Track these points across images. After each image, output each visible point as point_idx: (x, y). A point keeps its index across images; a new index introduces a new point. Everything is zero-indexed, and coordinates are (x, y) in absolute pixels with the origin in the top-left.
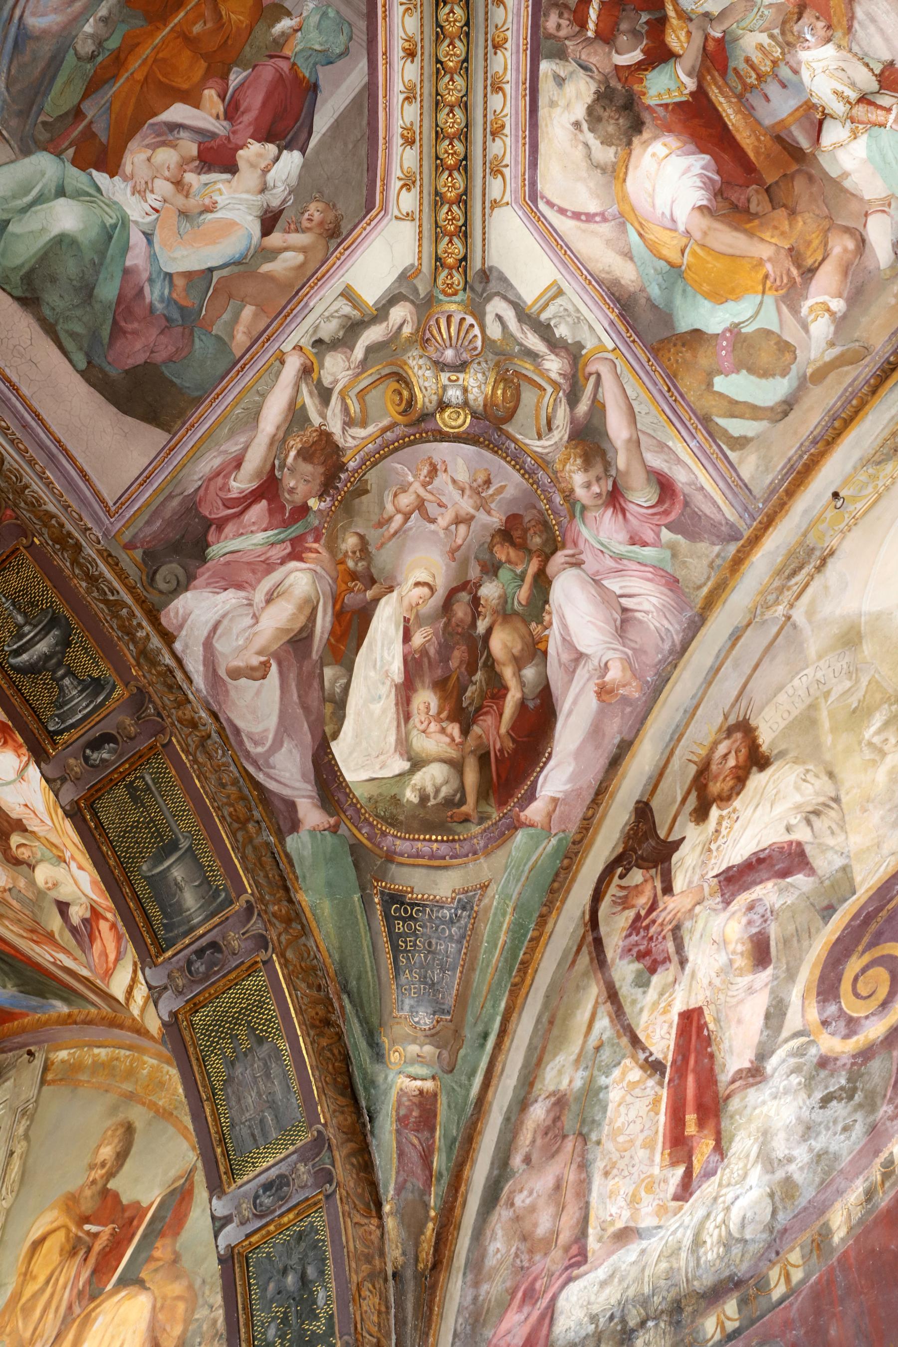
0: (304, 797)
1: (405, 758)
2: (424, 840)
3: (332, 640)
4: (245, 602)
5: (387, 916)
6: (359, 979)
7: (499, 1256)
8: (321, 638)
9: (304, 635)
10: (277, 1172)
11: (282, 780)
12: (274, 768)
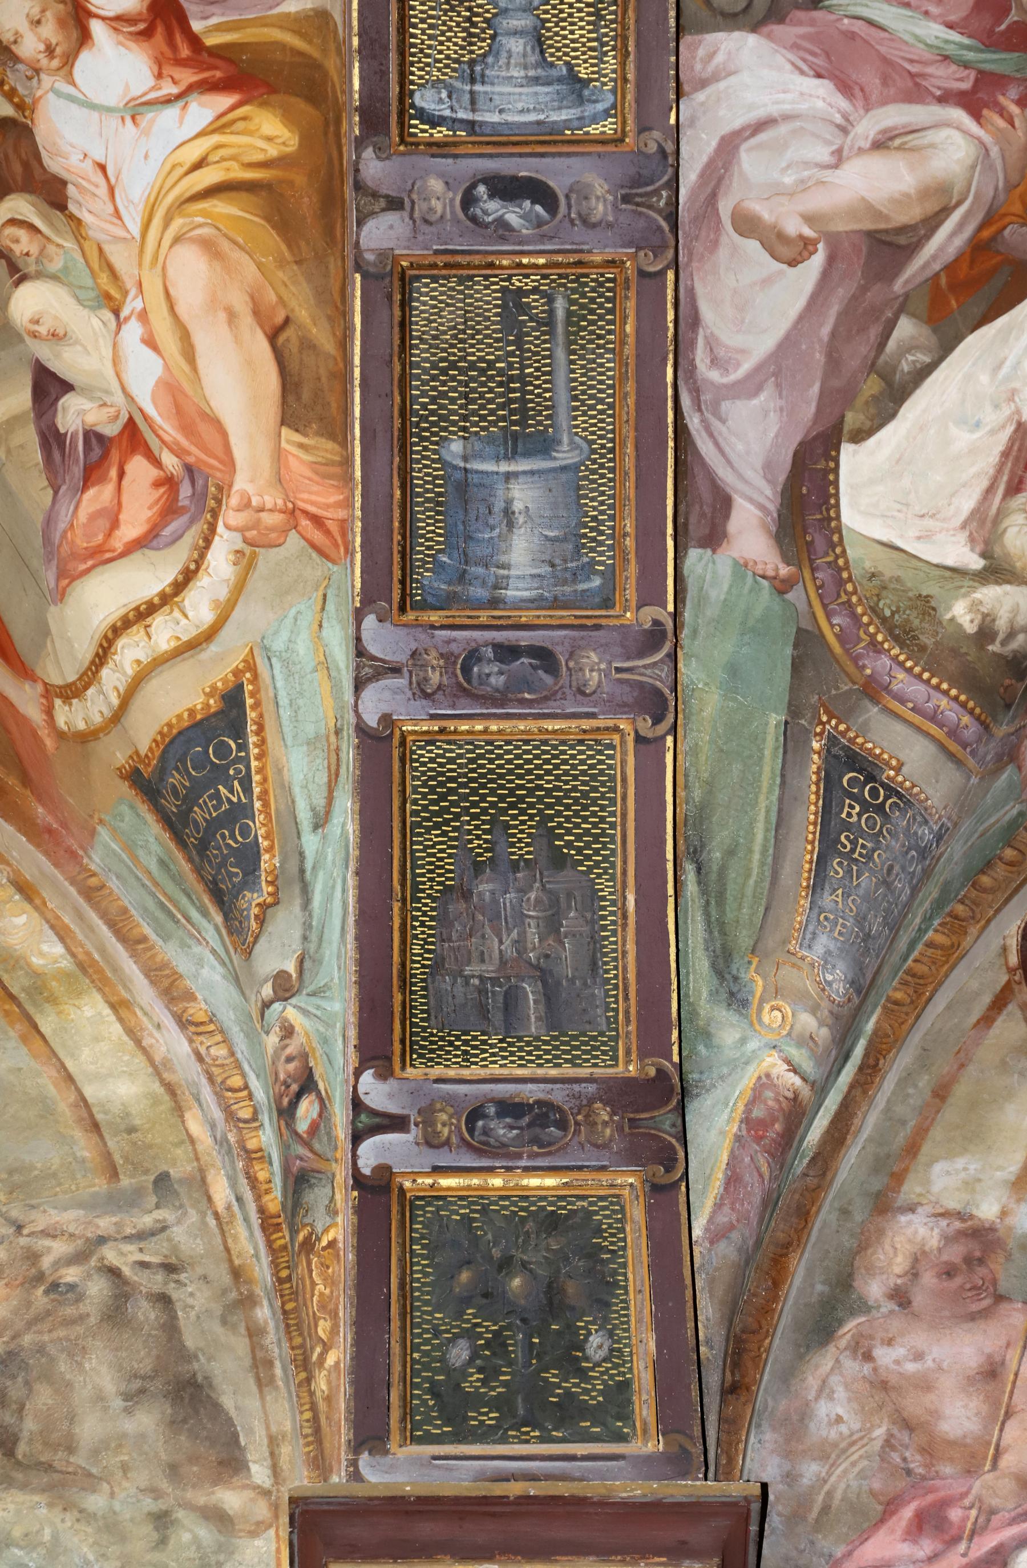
0: (751, 500)
1: (979, 548)
2: (956, 699)
3: (943, 281)
4: (838, 119)
5: (830, 782)
6: (730, 852)
7: (843, 1429)
8: (926, 265)
9: (902, 240)
10: (541, 1096)
11: (727, 449)
12: (723, 421)
